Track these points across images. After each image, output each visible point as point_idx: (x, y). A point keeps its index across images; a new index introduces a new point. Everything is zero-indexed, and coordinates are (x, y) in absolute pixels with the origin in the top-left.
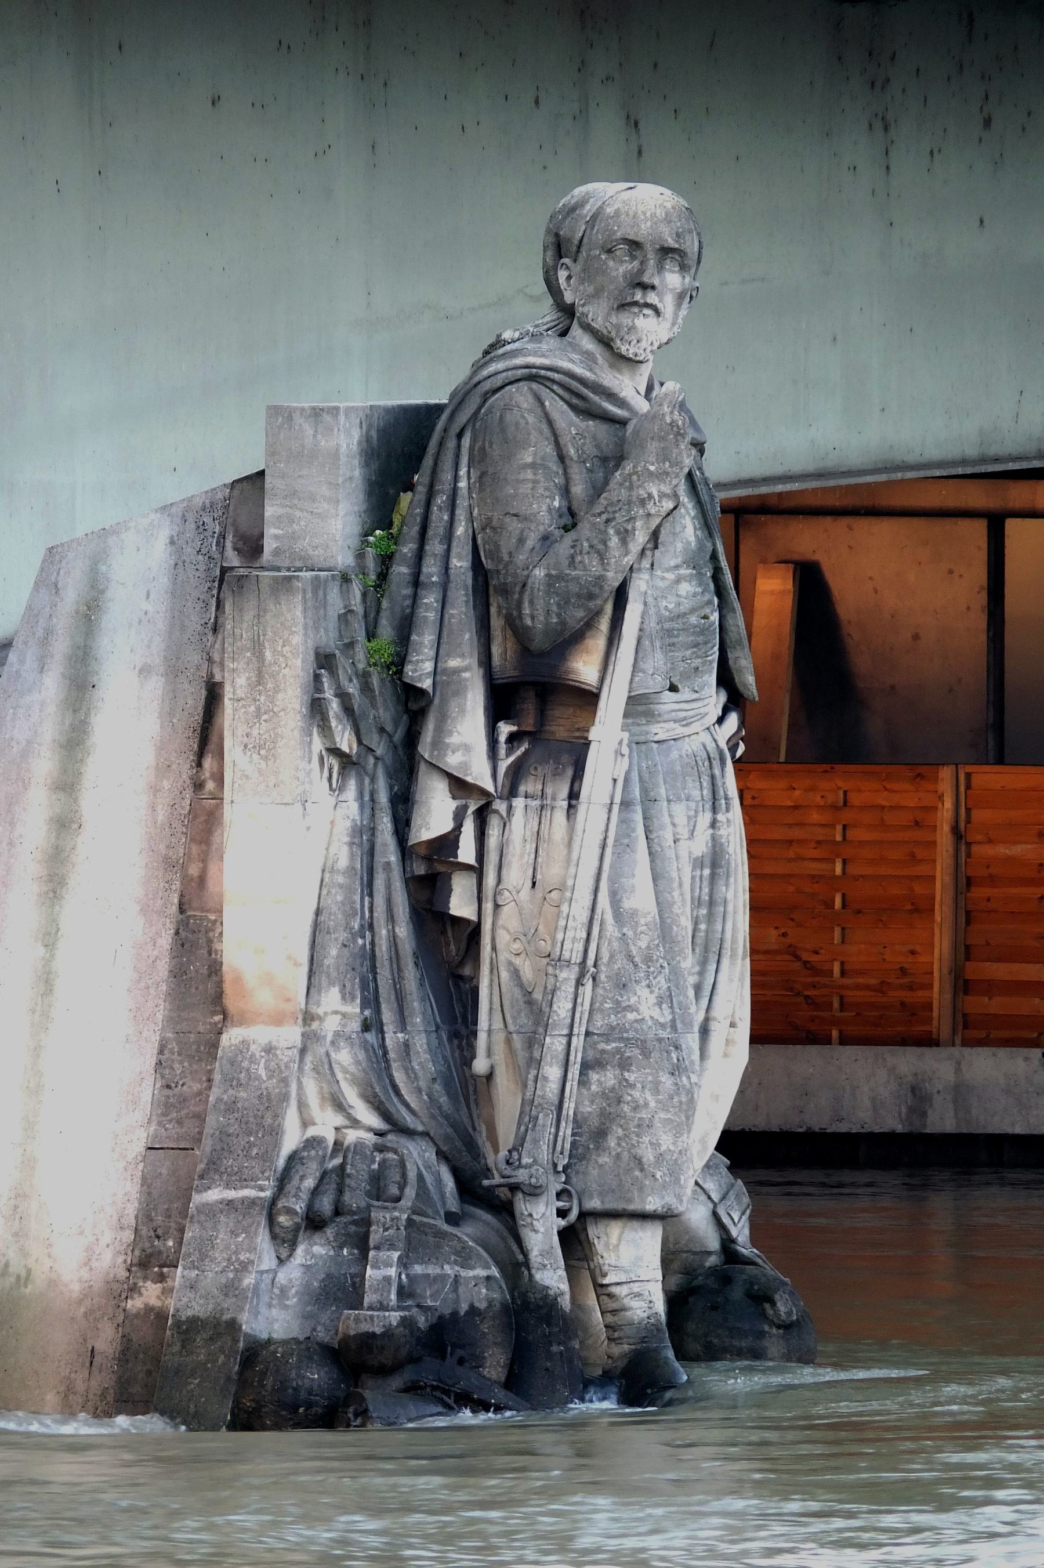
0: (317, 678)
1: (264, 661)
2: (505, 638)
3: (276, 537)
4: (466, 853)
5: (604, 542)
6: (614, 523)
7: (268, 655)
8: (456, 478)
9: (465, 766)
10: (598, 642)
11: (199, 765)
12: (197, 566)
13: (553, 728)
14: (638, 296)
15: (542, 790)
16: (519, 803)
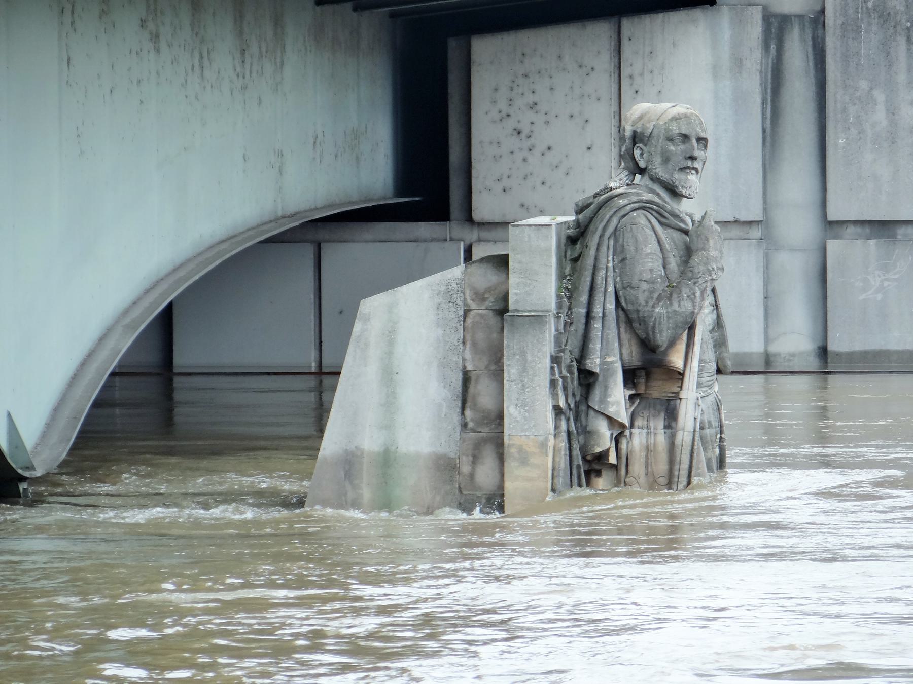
0: (552, 368)
4: (612, 459)
8: (608, 262)
9: (618, 413)
10: (681, 346)
11: (463, 413)
14: (689, 163)
16: (636, 431)
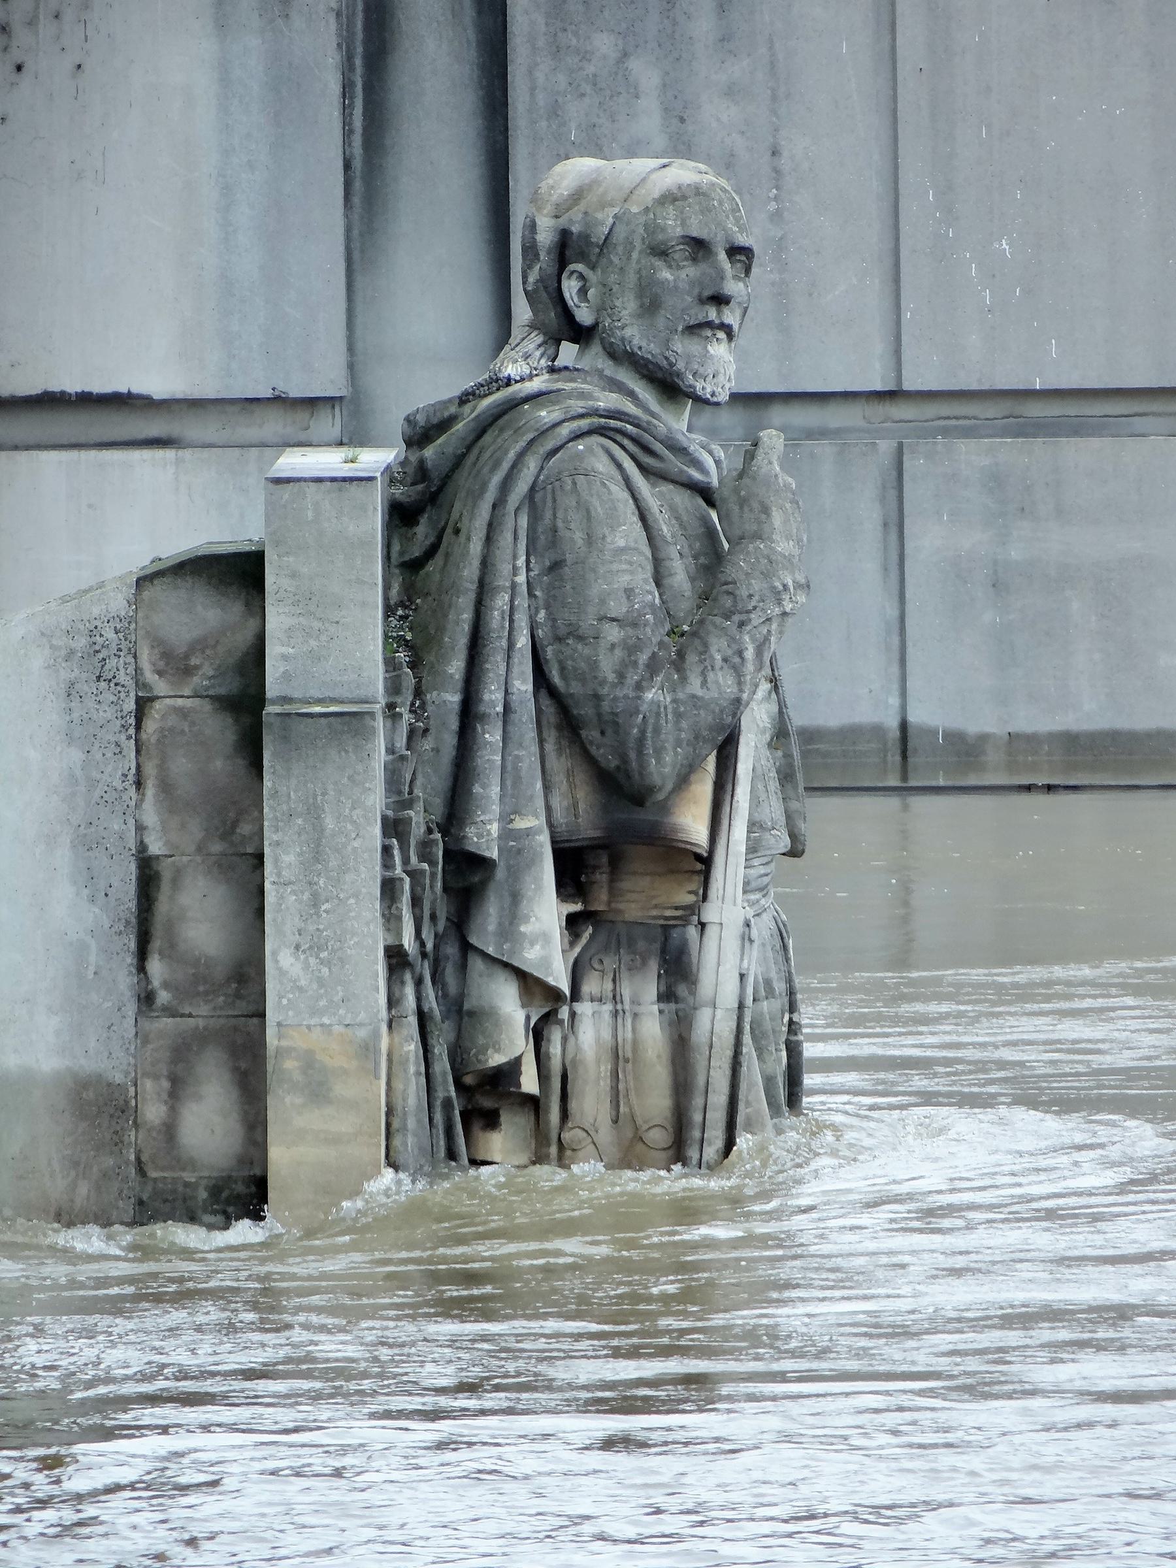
0: (386, 850)
1: (323, 830)
2: (572, 786)
3: (285, 658)
5: (740, 653)
6: (748, 628)
7: (330, 823)
11: (141, 968)
12: (100, 698)
13: (621, 906)
14: (712, 314)
15: (614, 990)
